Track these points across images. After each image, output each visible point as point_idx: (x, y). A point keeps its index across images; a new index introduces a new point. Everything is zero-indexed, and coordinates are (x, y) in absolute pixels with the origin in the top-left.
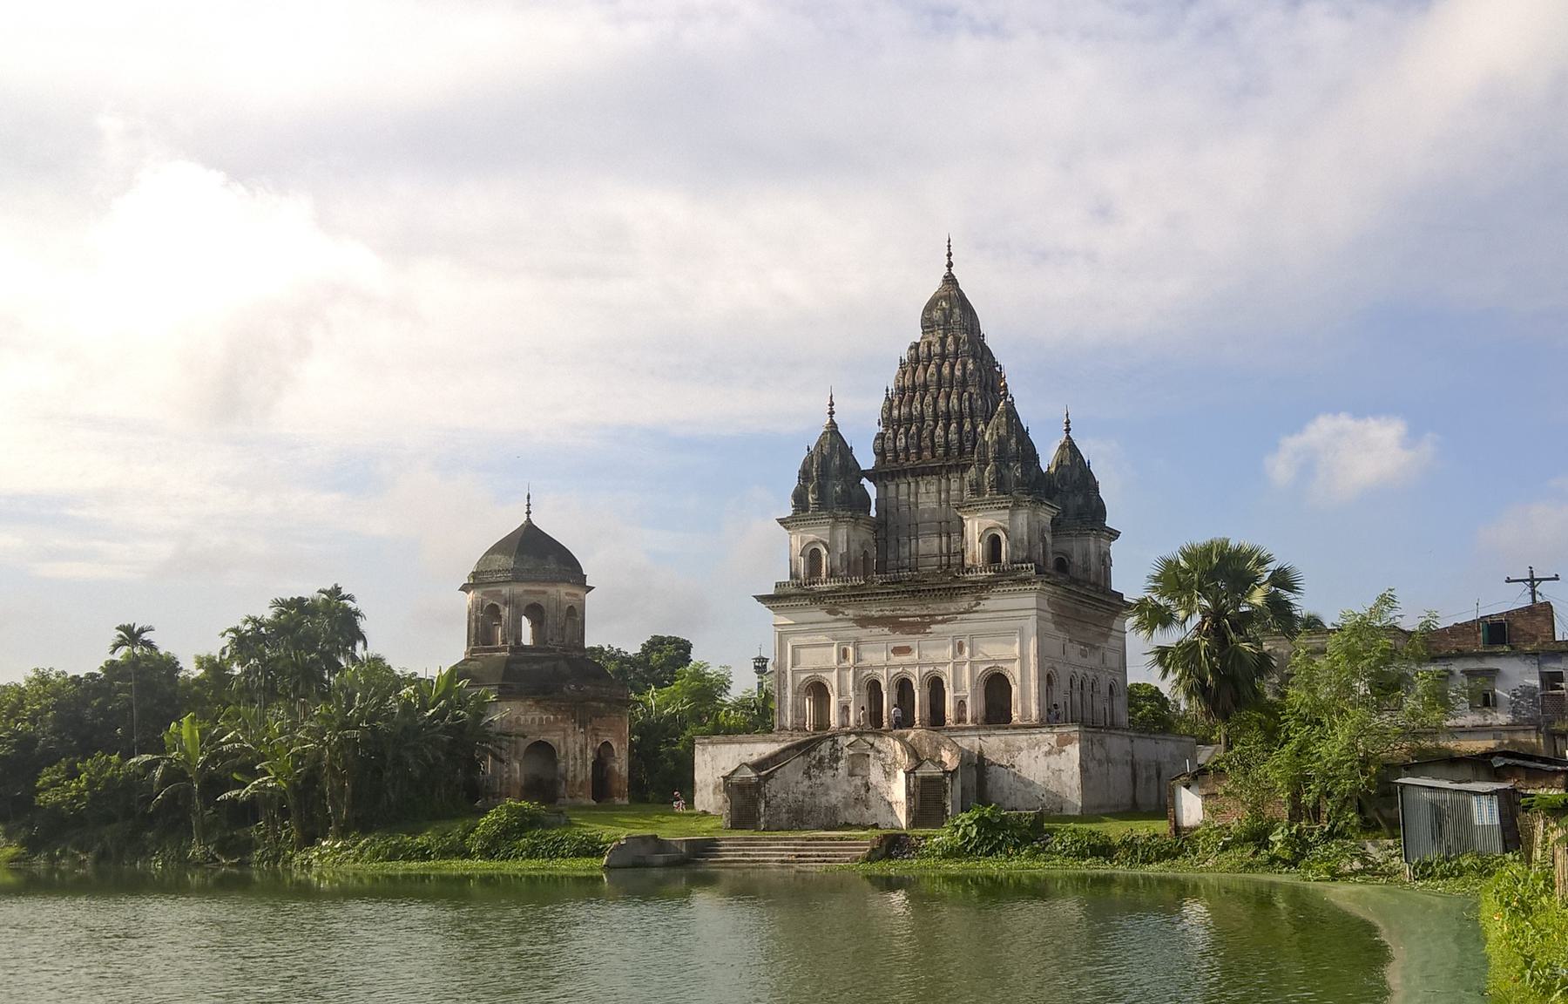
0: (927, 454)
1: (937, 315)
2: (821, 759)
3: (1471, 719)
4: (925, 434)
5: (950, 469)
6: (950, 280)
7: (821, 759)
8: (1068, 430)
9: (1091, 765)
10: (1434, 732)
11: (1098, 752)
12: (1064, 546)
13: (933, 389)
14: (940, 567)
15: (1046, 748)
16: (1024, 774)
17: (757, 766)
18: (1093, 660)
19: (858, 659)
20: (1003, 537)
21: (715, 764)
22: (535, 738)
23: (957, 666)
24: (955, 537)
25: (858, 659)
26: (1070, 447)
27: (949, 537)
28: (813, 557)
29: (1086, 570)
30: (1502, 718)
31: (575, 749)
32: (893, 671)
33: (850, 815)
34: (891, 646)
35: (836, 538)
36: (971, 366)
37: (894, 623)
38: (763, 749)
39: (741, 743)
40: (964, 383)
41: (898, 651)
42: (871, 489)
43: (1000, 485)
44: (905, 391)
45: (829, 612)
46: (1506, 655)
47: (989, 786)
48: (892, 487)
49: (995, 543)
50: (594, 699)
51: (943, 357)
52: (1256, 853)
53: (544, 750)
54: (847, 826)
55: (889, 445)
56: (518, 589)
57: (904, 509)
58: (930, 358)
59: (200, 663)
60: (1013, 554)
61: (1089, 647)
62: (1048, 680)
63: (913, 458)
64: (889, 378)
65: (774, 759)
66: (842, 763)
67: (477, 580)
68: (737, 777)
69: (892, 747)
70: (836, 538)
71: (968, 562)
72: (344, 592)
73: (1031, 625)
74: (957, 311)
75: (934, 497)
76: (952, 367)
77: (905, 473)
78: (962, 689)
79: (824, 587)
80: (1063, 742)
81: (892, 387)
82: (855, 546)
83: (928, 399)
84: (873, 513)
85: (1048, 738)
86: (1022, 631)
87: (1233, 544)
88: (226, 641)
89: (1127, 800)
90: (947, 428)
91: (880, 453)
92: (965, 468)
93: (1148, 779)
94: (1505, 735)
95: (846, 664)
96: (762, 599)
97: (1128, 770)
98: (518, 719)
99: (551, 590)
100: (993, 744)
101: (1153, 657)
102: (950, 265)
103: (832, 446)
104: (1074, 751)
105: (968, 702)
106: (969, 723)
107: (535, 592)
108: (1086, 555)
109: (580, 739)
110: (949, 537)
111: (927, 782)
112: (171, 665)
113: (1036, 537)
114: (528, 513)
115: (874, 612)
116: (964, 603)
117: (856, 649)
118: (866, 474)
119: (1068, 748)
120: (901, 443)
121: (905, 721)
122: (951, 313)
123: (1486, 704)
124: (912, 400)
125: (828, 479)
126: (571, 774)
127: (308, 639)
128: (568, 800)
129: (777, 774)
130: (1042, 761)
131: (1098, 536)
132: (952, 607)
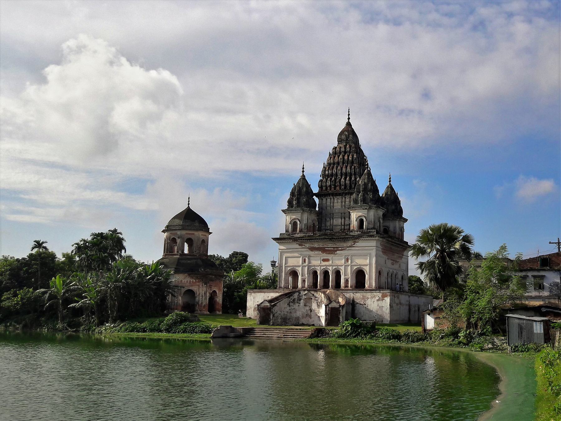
0: (338, 188)
1: (343, 137)
2: (294, 300)
3: (534, 294)
4: (337, 180)
5: (346, 194)
6: (349, 124)
7: (294, 300)
8: (390, 181)
9: (394, 305)
10: (521, 298)
11: (397, 301)
12: (387, 224)
13: (341, 164)
14: (341, 230)
15: (378, 298)
16: (369, 307)
17: (270, 301)
19: (309, 262)
20: (365, 220)
21: (255, 300)
23: (346, 267)
24: (347, 219)
25: (309, 262)
26: (390, 188)
28: (294, 225)
29: (395, 233)
30: (546, 293)
31: (202, 292)
32: (322, 268)
33: (304, 321)
34: (322, 258)
35: (304, 218)
36: (355, 156)
37: (323, 250)
38: (273, 295)
39: (265, 292)
40: (352, 162)
41: (324, 260)
42: (316, 199)
43: (364, 201)
44: (330, 165)
46: (548, 270)
47: (356, 312)
48: (324, 200)
50: (210, 275)
51: (345, 152)
52: (453, 340)
53: (191, 293)
54: (303, 325)
55: (324, 184)
56: (184, 232)
57: (329, 208)
58: (340, 153)
59: (64, 256)
60: (368, 226)
61: (395, 262)
62: (379, 273)
63: (333, 189)
64: (324, 159)
65: (276, 299)
66: (302, 301)
67: (168, 229)
69: (321, 296)
70: (304, 218)
71: (352, 228)
72: (118, 231)
73: (374, 253)
74: (351, 136)
75: (340, 204)
76: (348, 156)
77: (328, 195)
78: (347, 276)
80: (384, 296)
81: (326, 163)
82: (310, 221)
83: (339, 168)
84: (317, 209)
85: (379, 295)
86: (370, 254)
87: (449, 225)
88: (73, 248)
89: (407, 319)
90: (345, 179)
91: (321, 187)
92: (351, 194)
93: (415, 311)
94: (547, 300)
95: (305, 264)
96: (275, 239)
97: (408, 307)
98: (181, 281)
100: (358, 296)
101: (418, 266)
102: (349, 119)
103: (303, 184)
104: (388, 300)
105: (349, 280)
106: (349, 288)
107: (190, 234)
108: (395, 227)
109: (205, 289)
111: (333, 309)
112: (53, 256)
113: (377, 221)
114: (189, 204)
115: (316, 245)
116: (350, 243)
117: (309, 259)
118: (315, 194)
119: (386, 298)
120: (329, 183)
121: (326, 285)
122: (349, 136)
123: (540, 288)
124: (333, 168)
126: (200, 302)
127: (104, 248)
128: (199, 312)
129: (278, 305)
130: (376, 303)
131: (400, 221)
132: (345, 245)
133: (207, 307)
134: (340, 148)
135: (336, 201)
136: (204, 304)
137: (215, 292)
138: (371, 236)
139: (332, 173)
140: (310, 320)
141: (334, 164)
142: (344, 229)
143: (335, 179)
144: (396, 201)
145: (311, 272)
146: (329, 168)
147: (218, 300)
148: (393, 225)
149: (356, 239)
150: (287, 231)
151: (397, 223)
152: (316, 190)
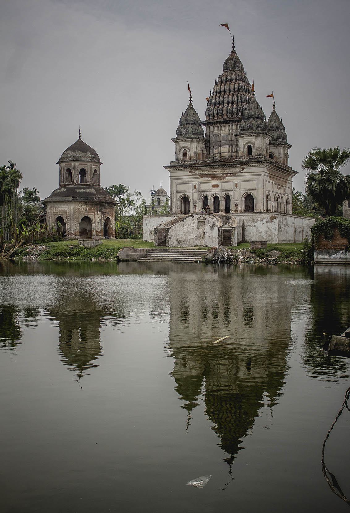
0: (225, 116)
5: (233, 121)
6: (233, 52)
8: (274, 108)
12: (273, 150)
13: (227, 93)
18: (281, 191)
21: (149, 226)
27: (232, 146)
37: (213, 176)
41: (214, 186)
45: (190, 172)
47: (246, 233)
48: (212, 128)
49: (250, 148)
53: (87, 220)
55: (211, 113)
57: (216, 136)
58: (226, 81)
61: (280, 186)
75: (227, 132)
76: (235, 84)
79: (189, 163)
81: (212, 91)
85: (268, 217)
89: (292, 239)
91: (208, 116)
93: (300, 232)
96: (166, 167)
99: (89, 164)
102: (233, 47)
108: (280, 153)
110: (232, 146)
111: (225, 231)
113: (264, 147)
116: (238, 170)
119: (274, 220)
120: (216, 112)
121: (216, 209)
128: (96, 237)
129: (173, 228)
130: (265, 225)
132: (234, 171)
133: (103, 232)
135: (223, 129)
138: (259, 162)
141: (220, 92)
144: (280, 128)
145: (202, 198)
148: (278, 152)
150: (177, 159)
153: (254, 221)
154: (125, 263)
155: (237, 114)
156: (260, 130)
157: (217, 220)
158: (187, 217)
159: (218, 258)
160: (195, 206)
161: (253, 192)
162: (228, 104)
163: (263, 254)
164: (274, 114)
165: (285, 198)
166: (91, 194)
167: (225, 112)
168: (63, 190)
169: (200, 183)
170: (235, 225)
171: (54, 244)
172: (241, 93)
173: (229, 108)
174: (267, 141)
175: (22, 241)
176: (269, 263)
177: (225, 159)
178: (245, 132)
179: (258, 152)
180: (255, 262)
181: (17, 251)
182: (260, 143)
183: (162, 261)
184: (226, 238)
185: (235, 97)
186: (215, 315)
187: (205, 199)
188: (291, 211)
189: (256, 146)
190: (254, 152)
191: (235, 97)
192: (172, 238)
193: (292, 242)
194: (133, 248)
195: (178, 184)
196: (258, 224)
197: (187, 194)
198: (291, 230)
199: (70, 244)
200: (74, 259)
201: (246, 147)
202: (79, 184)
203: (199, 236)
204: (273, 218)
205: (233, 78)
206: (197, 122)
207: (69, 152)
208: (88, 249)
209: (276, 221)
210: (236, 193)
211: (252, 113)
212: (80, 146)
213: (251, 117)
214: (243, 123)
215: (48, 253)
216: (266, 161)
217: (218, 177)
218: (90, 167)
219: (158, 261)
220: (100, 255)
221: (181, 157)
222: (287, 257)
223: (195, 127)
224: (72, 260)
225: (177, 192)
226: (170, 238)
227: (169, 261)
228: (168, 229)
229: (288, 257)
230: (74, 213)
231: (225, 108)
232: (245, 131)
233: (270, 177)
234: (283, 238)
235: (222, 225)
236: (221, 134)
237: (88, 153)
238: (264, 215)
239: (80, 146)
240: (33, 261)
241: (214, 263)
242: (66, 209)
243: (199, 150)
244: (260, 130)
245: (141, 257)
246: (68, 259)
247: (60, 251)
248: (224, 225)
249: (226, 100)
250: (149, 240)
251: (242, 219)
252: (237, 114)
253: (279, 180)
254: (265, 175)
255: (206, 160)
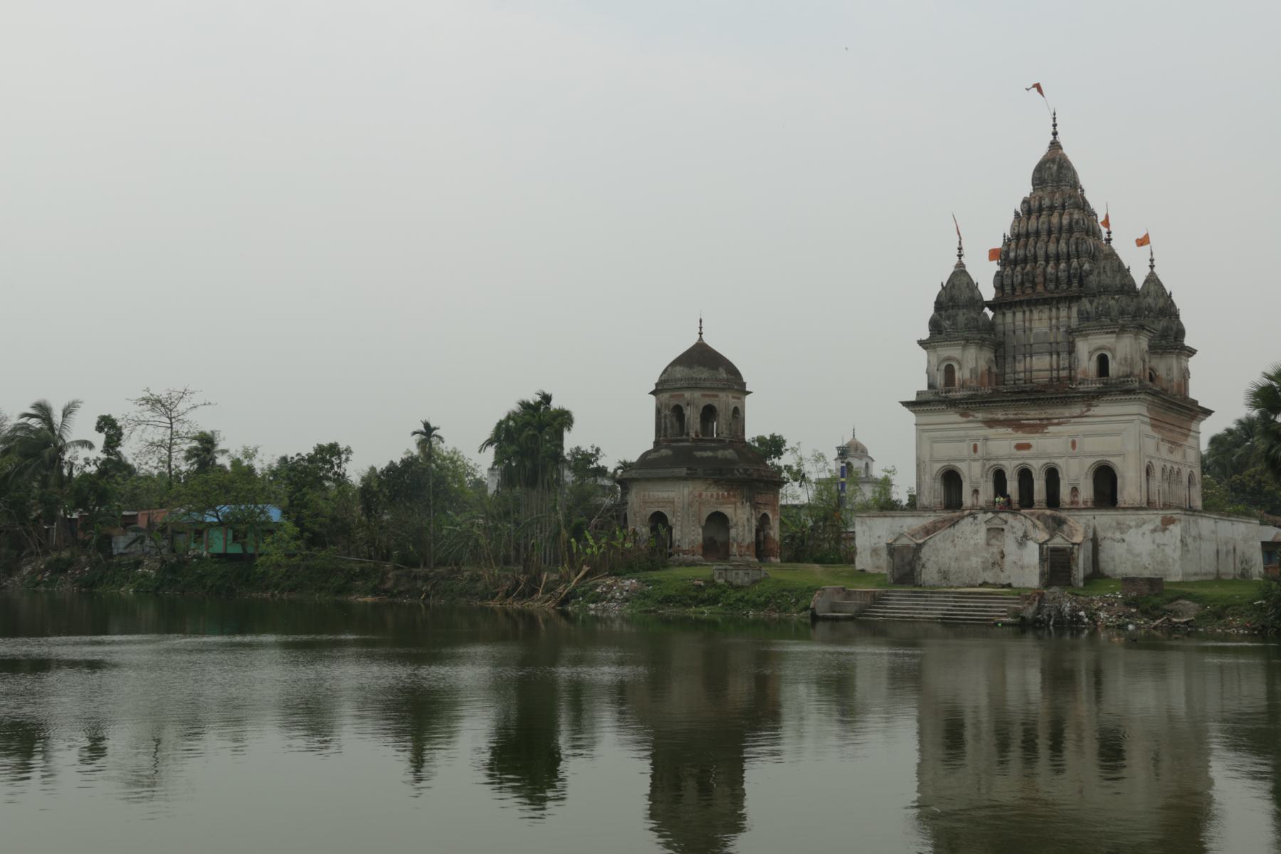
0: (1040, 288)
5: (1059, 300)
6: (1055, 145)
13: (1044, 237)
14: (1051, 379)
15: (1152, 527)
18: (1177, 456)
21: (871, 537)
22: (714, 510)
27: (1058, 355)
28: (949, 371)
37: (1016, 425)
41: (1020, 447)
45: (962, 415)
48: (1009, 316)
49: (1103, 362)
53: (718, 520)
55: (1007, 281)
57: (1019, 332)
58: (1040, 209)
61: (1174, 444)
68: (899, 543)
75: (1046, 323)
76: (1061, 216)
77: (1021, 303)
78: (1077, 477)
81: (1008, 234)
85: (1155, 518)
93: (1227, 553)
96: (906, 404)
99: (722, 395)
102: (1055, 134)
108: (1170, 369)
110: (1058, 355)
113: (1137, 358)
115: (1000, 416)
116: (1076, 410)
119: (1171, 527)
120: (1018, 279)
121: (1027, 499)
125: (954, 309)
126: (740, 539)
129: (931, 542)
131: (1179, 355)
132: (1067, 412)
133: (753, 548)
134: (1041, 199)
135: (1036, 315)
136: (748, 541)
137: (765, 516)
139: (1026, 255)
140: (1002, 575)
141: (1027, 235)
142: (1058, 378)
143: (1034, 268)
144: (1168, 311)
146: (1017, 245)
147: (772, 533)
148: (1165, 366)
149: (1093, 398)
150: (931, 386)
151: (1173, 361)
152: (988, 293)
153: (1121, 527)
154: (828, 624)
155: (1069, 283)
156: (1128, 319)
157: (1035, 526)
158: (963, 518)
159: (1050, 616)
160: (976, 492)
161: (1116, 462)
162: (1047, 261)
163: (1156, 607)
164: (1152, 279)
165: (1185, 472)
166: (727, 461)
167: (1039, 279)
168: (664, 452)
169: (986, 439)
170: (1078, 538)
171: (655, 575)
172: (1076, 235)
173: (1049, 270)
174: (1144, 342)
175: (586, 569)
176: (1173, 628)
177: (1045, 386)
178: (1091, 323)
179: (1126, 370)
180: (1138, 627)
181: (574, 590)
182: (1126, 349)
183: (914, 621)
184: (1057, 565)
185: (1063, 245)
186: (1029, 746)
187: (999, 478)
188: (1198, 503)
189: (1119, 355)
190: (1113, 368)
191: (1063, 245)
192: (928, 565)
193: (1210, 578)
194: (843, 589)
195: (935, 440)
196: (1132, 535)
197: (958, 465)
198: (1208, 548)
199: (695, 578)
200: (706, 611)
201: (1095, 358)
202: (701, 440)
203: (991, 561)
204: (1167, 522)
205: (1058, 202)
206: (976, 302)
207: (678, 368)
208: (738, 588)
209: (1176, 529)
210: (1074, 463)
211: (1106, 280)
212: (702, 360)
213: (1105, 290)
214: (1085, 303)
215: (646, 596)
216: (1144, 389)
217: (1029, 425)
218: (724, 401)
219: (903, 620)
220: (766, 603)
221: (940, 380)
222: (1219, 615)
223: (973, 314)
224: (703, 613)
225: (934, 461)
226: (923, 566)
227: (931, 620)
228: (920, 546)
229: (1220, 618)
230: (690, 505)
231: (1039, 271)
232: (1089, 324)
233: (1152, 425)
234: (1192, 568)
235: (1047, 537)
236: (1031, 330)
237: (721, 370)
238: (1144, 515)
239: (702, 360)
240: (612, 615)
241: (1040, 628)
242: (672, 494)
243: (983, 366)
244: (1128, 319)
245: (862, 611)
246: (692, 611)
247: (673, 593)
248: (1052, 537)
249: (1041, 253)
250: (869, 569)
251: (1091, 523)
252: (1069, 283)
253: (1171, 431)
254: (1143, 422)
255: (1001, 387)
